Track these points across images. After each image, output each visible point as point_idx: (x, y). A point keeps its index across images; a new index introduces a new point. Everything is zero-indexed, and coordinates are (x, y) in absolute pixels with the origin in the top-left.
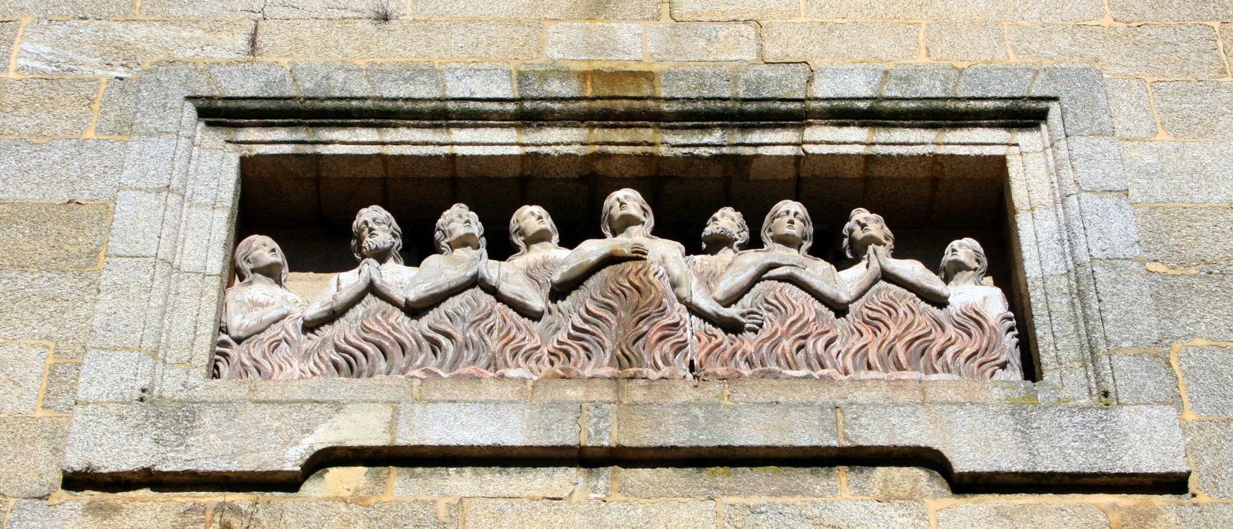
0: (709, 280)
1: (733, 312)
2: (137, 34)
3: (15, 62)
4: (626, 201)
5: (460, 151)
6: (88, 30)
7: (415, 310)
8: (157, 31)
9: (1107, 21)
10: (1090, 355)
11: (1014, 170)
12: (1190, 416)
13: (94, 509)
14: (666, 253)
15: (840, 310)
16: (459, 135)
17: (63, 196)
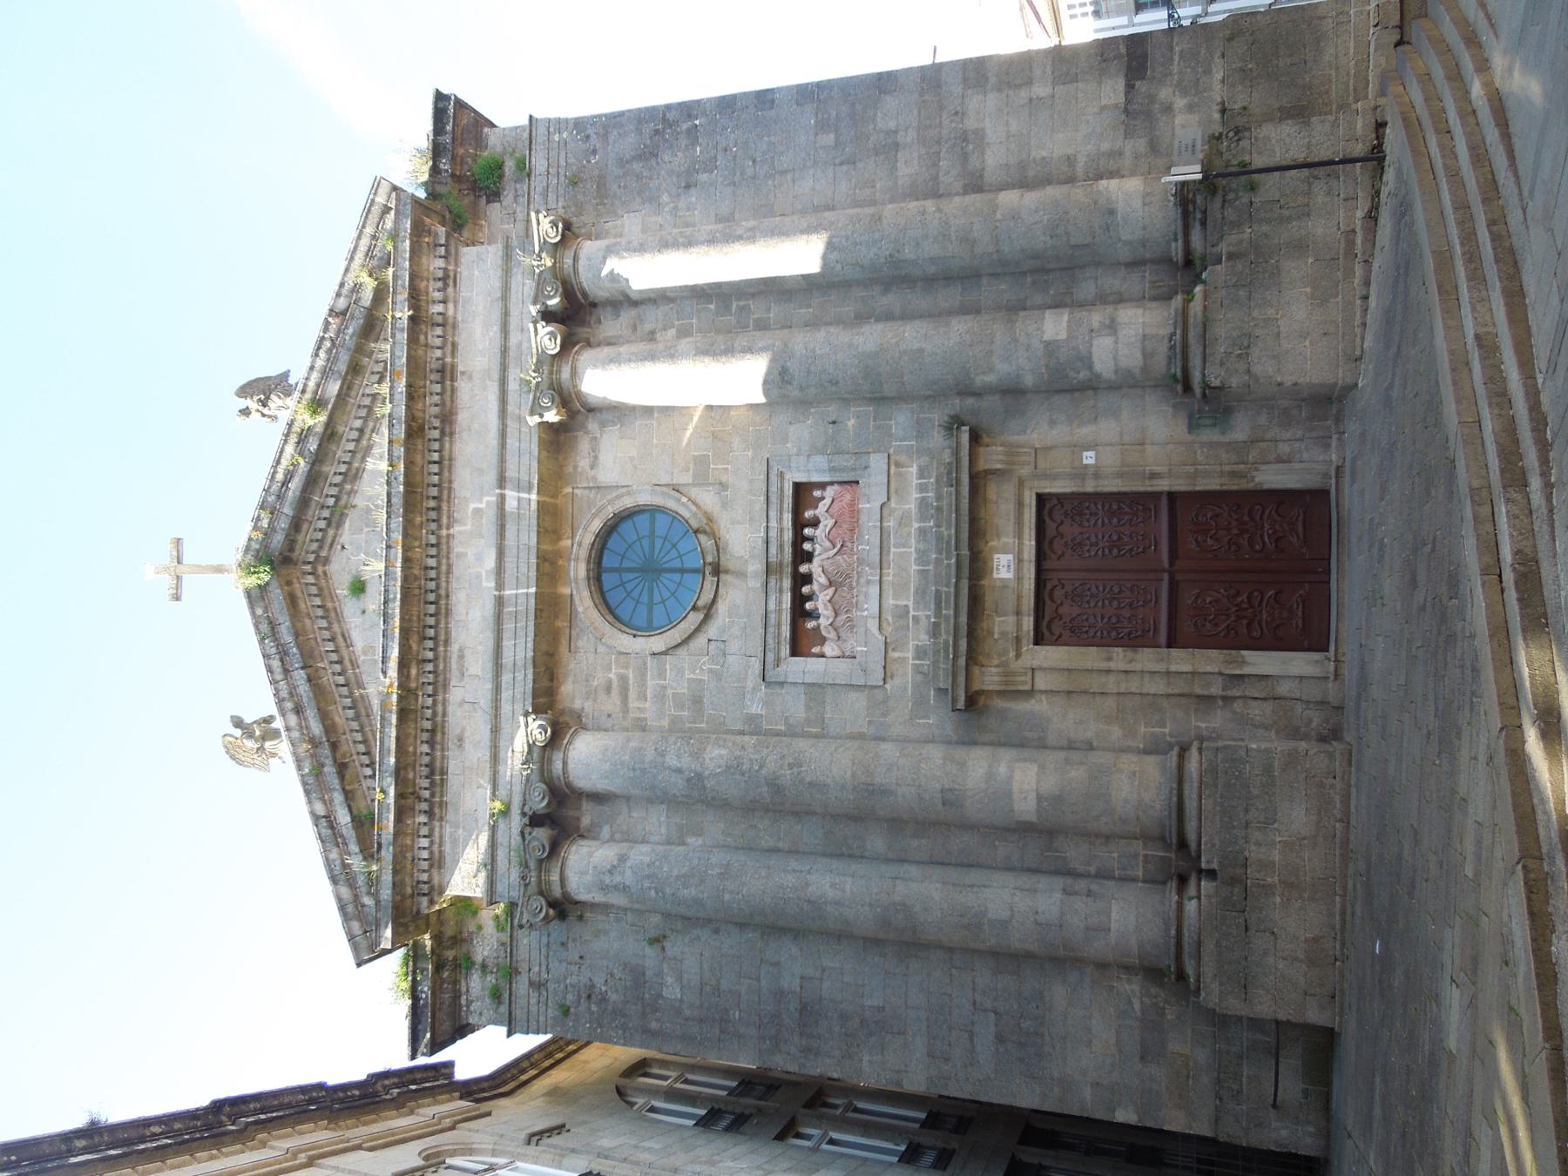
0: (826, 550)
1: (839, 546)
2: (750, 684)
3: (759, 712)
4: (803, 569)
5: (789, 606)
6: (748, 696)
7: (836, 614)
8: (749, 680)
9: (750, 453)
10: (854, 470)
11: (797, 480)
12: (871, 450)
13: (892, 677)
14: (816, 561)
15: (836, 522)
16: (784, 606)
17: (803, 696)
